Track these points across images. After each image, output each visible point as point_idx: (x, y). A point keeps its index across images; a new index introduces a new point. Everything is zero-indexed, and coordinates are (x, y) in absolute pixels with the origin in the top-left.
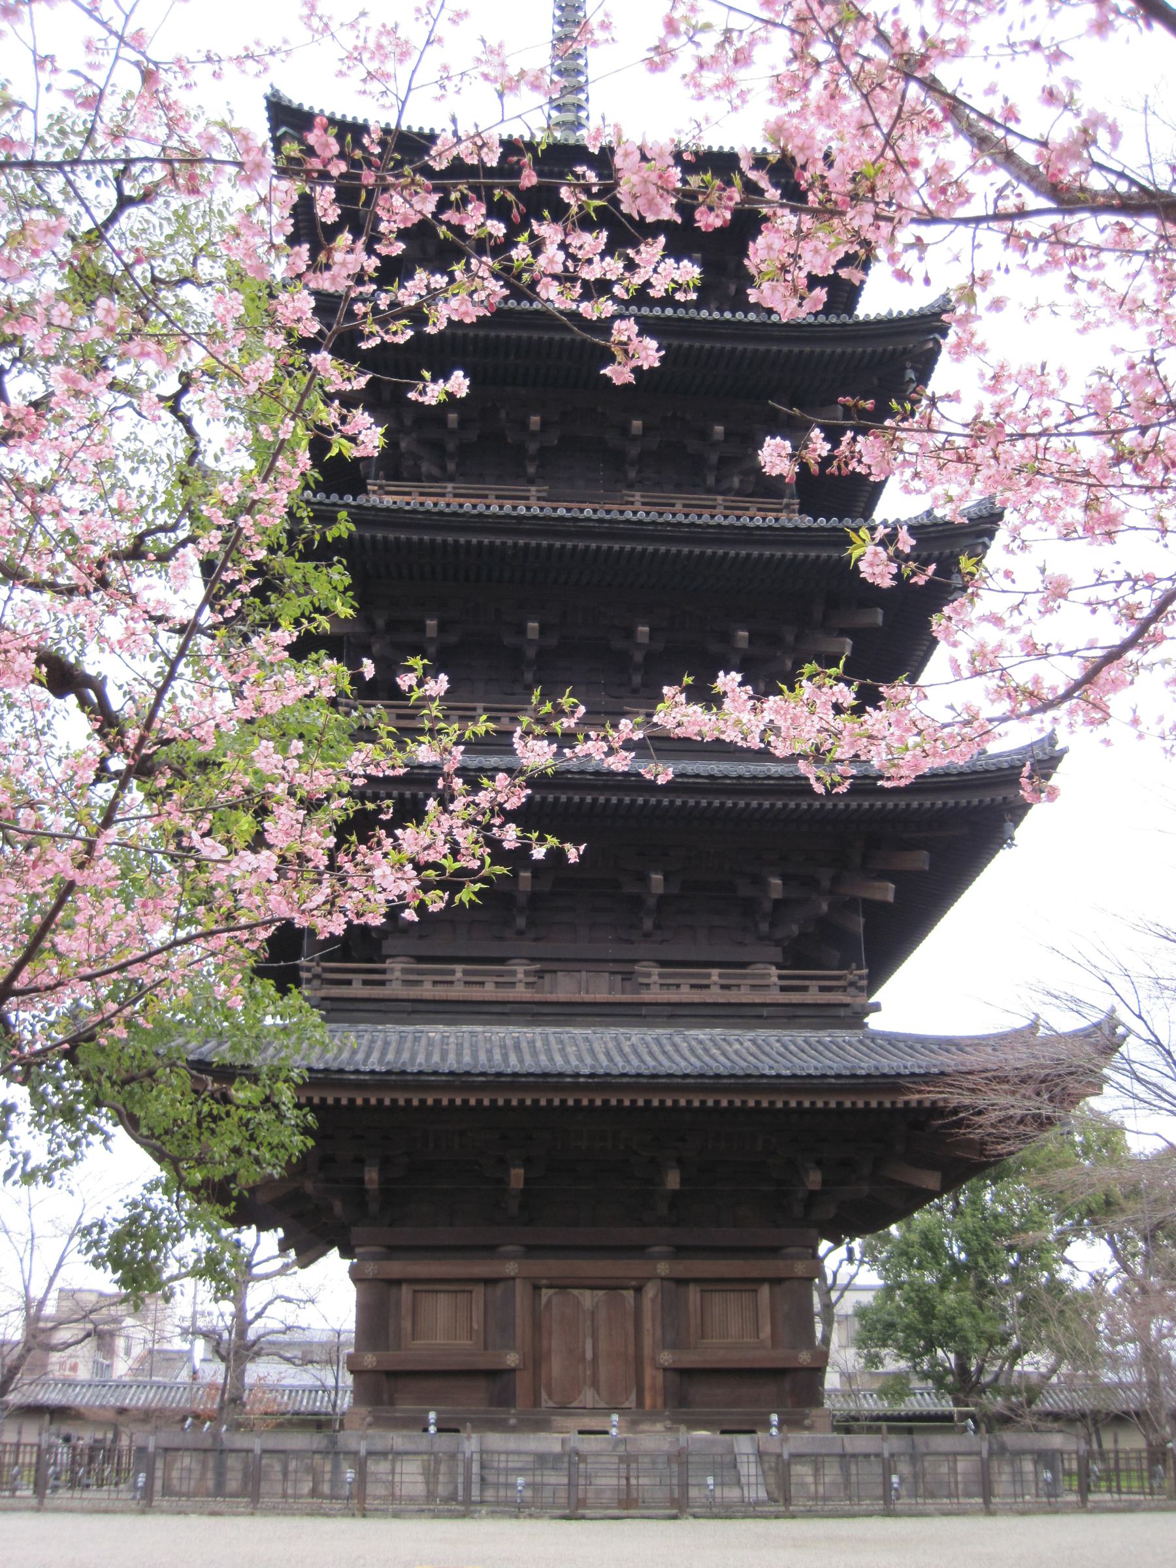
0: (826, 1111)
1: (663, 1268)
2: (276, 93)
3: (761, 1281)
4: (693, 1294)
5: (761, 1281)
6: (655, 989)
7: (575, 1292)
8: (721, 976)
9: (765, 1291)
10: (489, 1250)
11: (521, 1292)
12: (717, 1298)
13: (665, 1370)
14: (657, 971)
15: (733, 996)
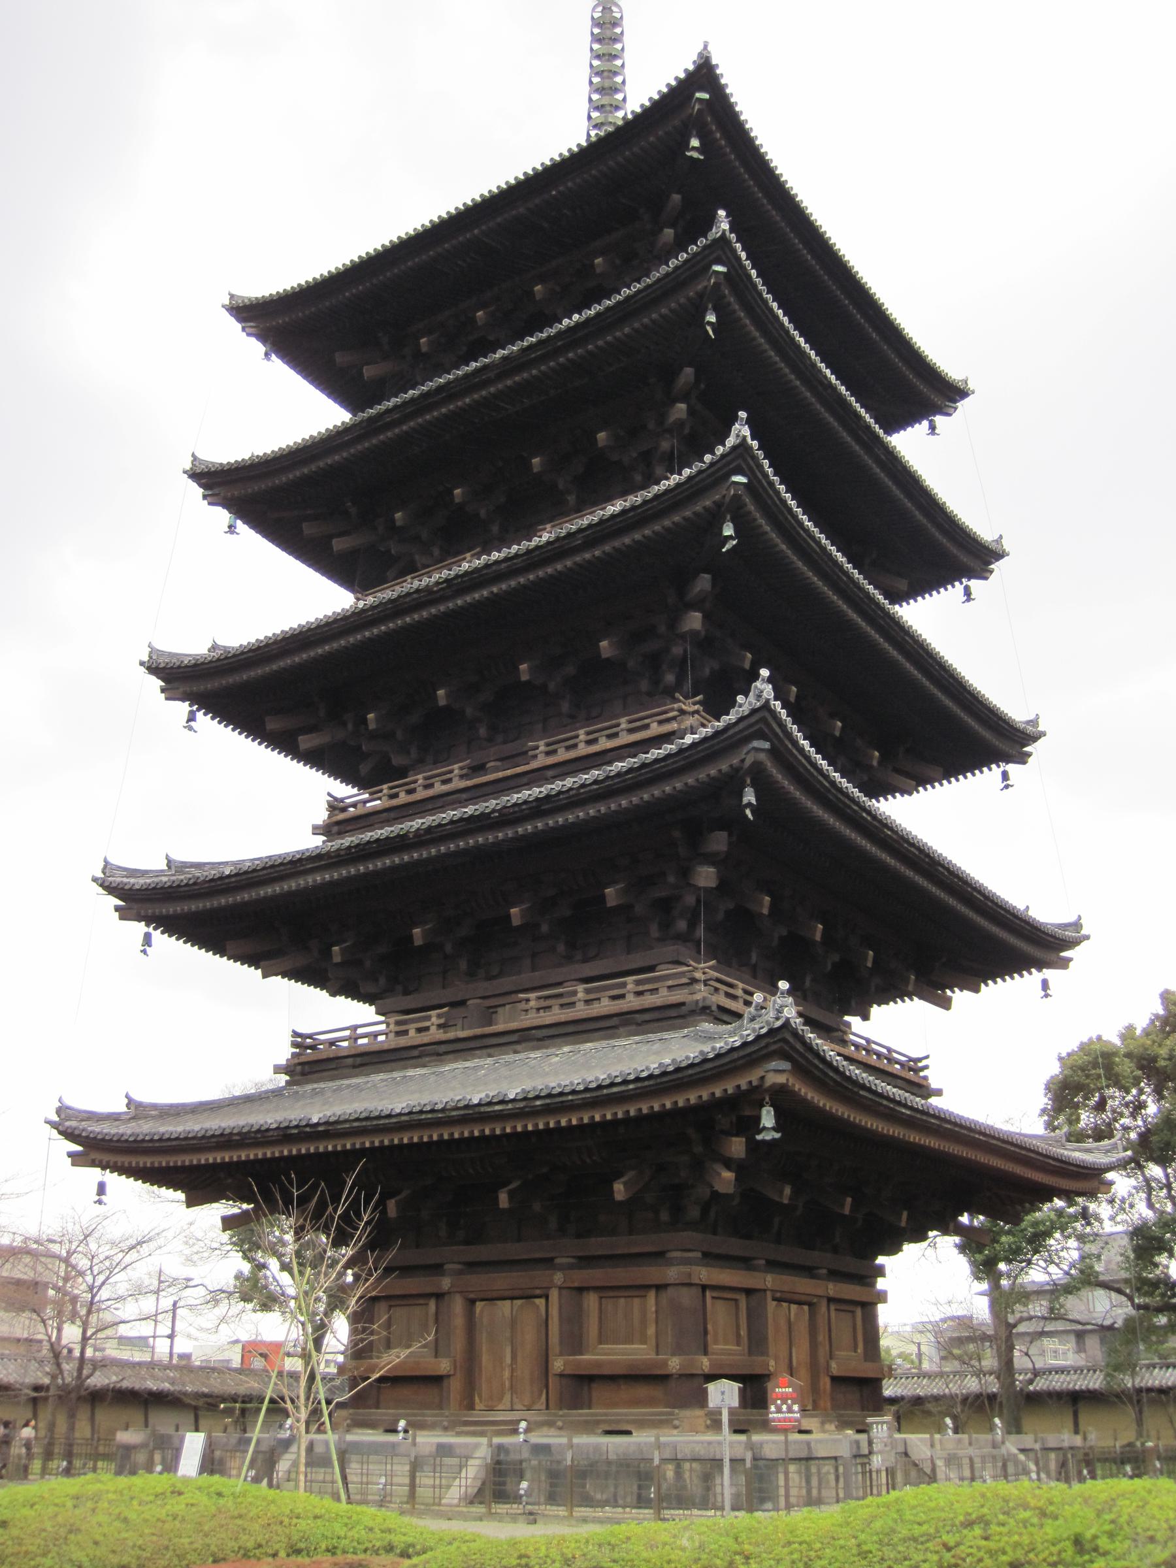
0: (615, 1122)
1: (558, 1278)
2: (232, 296)
3: (648, 1287)
4: (591, 1301)
5: (648, 1287)
6: (532, 1014)
7: (499, 1302)
8: (587, 991)
9: (652, 1294)
10: (436, 1269)
11: (458, 1305)
12: (609, 1305)
13: (561, 1375)
14: (580, 988)
15: (650, 1000)
